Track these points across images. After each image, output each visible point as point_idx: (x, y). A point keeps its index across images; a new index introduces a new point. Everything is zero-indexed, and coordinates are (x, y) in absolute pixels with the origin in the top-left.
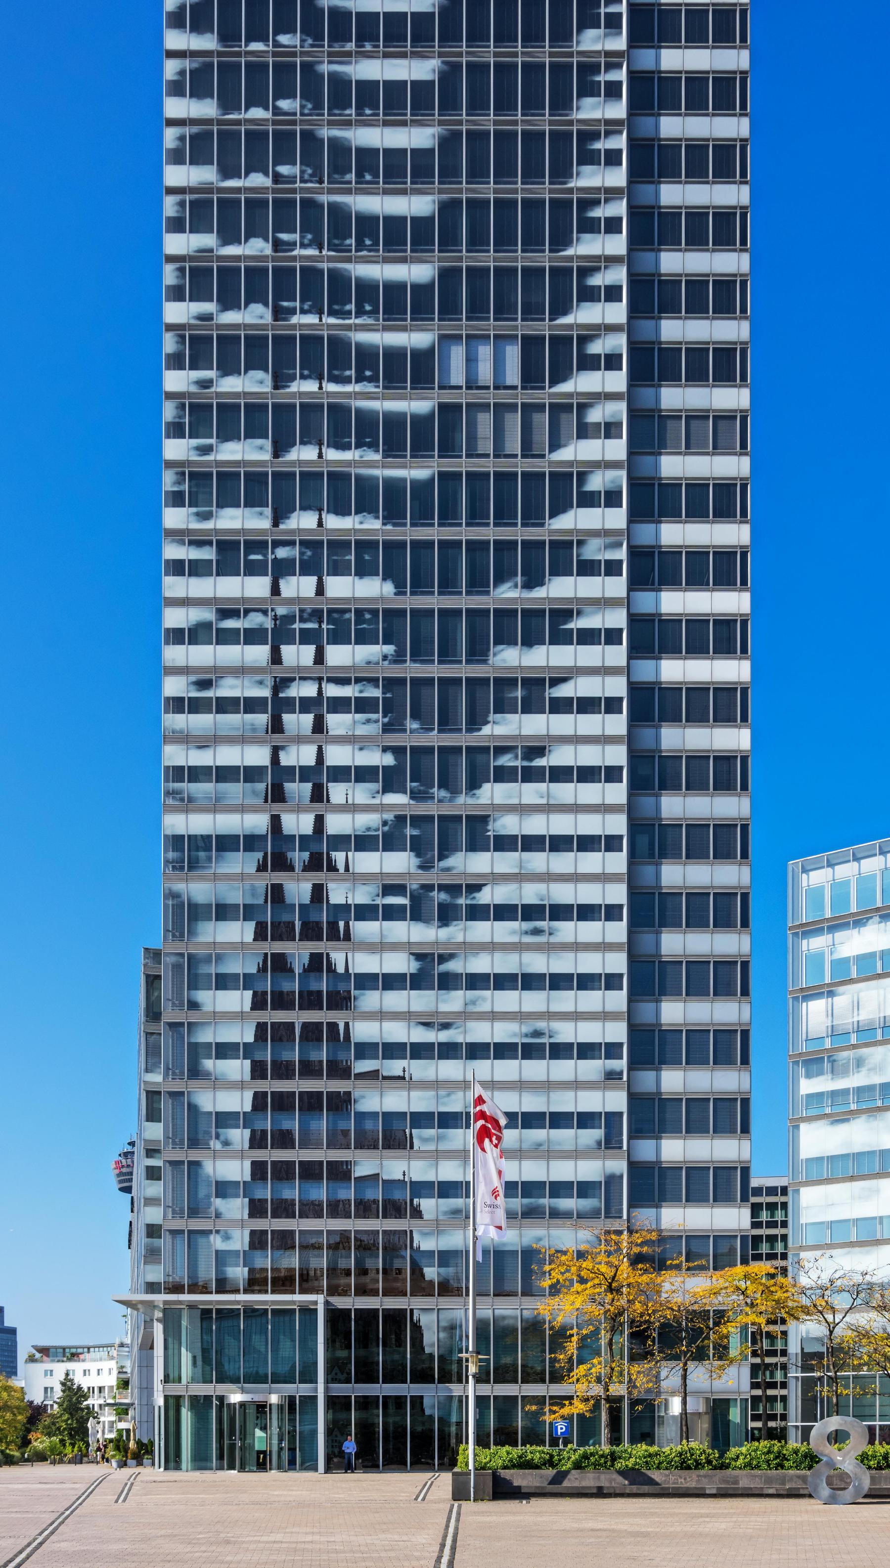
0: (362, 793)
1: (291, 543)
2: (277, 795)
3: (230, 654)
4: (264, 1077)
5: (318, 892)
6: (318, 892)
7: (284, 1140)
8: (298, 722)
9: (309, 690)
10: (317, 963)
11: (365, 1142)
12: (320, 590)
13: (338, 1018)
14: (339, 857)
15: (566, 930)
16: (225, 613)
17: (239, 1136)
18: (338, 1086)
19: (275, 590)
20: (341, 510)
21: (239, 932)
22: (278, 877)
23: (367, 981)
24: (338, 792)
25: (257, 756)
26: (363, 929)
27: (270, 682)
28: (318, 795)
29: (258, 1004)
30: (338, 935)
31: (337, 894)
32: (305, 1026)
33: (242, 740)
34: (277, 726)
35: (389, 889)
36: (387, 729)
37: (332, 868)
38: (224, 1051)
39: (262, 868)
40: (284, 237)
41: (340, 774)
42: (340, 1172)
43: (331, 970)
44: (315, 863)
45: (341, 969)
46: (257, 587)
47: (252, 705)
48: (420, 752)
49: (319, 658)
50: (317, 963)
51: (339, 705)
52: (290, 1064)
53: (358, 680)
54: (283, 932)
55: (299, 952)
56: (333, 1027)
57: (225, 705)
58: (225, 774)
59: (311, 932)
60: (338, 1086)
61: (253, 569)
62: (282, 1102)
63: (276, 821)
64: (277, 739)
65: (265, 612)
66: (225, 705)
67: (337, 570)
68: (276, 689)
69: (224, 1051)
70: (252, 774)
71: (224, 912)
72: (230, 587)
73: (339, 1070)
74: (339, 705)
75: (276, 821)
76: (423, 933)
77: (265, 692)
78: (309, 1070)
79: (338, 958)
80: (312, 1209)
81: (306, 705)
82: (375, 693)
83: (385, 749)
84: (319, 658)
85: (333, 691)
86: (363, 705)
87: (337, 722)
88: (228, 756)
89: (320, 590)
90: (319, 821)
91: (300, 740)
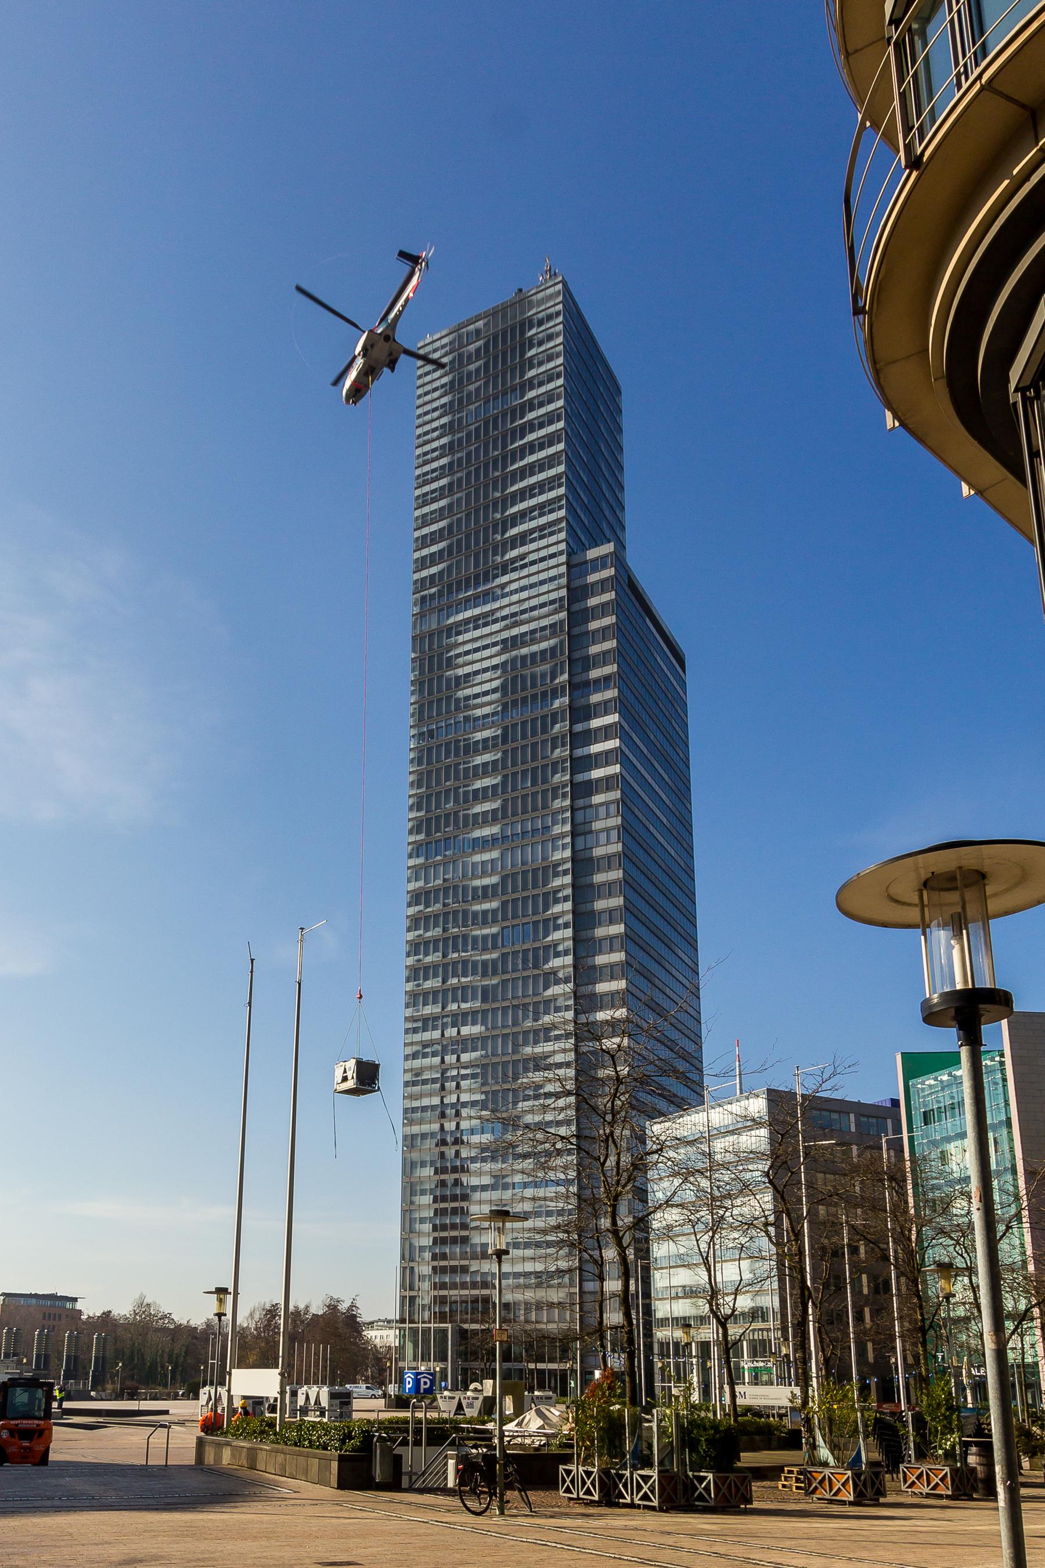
1: (448, 1016)
2: (443, 1115)
3: (427, 1061)
5: (457, 1153)
6: (457, 1153)
7: (444, 1256)
8: (451, 1085)
9: (454, 1073)
12: (459, 1032)
13: (464, 1204)
14: (465, 1138)
15: (479, 678)
16: (425, 1046)
19: (443, 1035)
20: (465, 1000)
21: (428, 1171)
22: (443, 1149)
24: (464, 1112)
25: (436, 1101)
26: (474, 1167)
28: (458, 1114)
29: (435, 1201)
30: (464, 1170)
31: (464, 1155)
32: (452, 1208)
33: (430, 1095)
34: (443, 1088)
36: (483, 1084)
37: (462, 1142)
39: (437, 1145)
41: (465, 1105)
43: (462, 1185)
44: (457, 1141)
46: (436, 1034)
47: (434, 1081)
48: (495, 1093)
50: (457, 1182)
51: (465, 1077)
52: (446, 1225)
54: (444, 1170)
55: (450, 1178)
57: (425, 1082)
58: (424, 1109)
59: (455, 1169)
61: (434, 1028)
62: (443, 1241)
63: (442, 1126)
64: (443, 1093)
66: (425, 1082)
67: (464, 1024)
68: (442, 1074)
70: (433, 1108)
71: (423, 1164)
72: (427, 1036)
74: (465, 1077)
75: (442, 1126)
78: (454, 1226)
79: (464, 1180)
81: (453, 1078)
83: (482, 1093)
85: (463, 1072)
86: (474, 1076)
87: (464, 1084)
88: (426, 1102)
89: (459, 1032)
90: (458, 1124)
91: (451, 1093)
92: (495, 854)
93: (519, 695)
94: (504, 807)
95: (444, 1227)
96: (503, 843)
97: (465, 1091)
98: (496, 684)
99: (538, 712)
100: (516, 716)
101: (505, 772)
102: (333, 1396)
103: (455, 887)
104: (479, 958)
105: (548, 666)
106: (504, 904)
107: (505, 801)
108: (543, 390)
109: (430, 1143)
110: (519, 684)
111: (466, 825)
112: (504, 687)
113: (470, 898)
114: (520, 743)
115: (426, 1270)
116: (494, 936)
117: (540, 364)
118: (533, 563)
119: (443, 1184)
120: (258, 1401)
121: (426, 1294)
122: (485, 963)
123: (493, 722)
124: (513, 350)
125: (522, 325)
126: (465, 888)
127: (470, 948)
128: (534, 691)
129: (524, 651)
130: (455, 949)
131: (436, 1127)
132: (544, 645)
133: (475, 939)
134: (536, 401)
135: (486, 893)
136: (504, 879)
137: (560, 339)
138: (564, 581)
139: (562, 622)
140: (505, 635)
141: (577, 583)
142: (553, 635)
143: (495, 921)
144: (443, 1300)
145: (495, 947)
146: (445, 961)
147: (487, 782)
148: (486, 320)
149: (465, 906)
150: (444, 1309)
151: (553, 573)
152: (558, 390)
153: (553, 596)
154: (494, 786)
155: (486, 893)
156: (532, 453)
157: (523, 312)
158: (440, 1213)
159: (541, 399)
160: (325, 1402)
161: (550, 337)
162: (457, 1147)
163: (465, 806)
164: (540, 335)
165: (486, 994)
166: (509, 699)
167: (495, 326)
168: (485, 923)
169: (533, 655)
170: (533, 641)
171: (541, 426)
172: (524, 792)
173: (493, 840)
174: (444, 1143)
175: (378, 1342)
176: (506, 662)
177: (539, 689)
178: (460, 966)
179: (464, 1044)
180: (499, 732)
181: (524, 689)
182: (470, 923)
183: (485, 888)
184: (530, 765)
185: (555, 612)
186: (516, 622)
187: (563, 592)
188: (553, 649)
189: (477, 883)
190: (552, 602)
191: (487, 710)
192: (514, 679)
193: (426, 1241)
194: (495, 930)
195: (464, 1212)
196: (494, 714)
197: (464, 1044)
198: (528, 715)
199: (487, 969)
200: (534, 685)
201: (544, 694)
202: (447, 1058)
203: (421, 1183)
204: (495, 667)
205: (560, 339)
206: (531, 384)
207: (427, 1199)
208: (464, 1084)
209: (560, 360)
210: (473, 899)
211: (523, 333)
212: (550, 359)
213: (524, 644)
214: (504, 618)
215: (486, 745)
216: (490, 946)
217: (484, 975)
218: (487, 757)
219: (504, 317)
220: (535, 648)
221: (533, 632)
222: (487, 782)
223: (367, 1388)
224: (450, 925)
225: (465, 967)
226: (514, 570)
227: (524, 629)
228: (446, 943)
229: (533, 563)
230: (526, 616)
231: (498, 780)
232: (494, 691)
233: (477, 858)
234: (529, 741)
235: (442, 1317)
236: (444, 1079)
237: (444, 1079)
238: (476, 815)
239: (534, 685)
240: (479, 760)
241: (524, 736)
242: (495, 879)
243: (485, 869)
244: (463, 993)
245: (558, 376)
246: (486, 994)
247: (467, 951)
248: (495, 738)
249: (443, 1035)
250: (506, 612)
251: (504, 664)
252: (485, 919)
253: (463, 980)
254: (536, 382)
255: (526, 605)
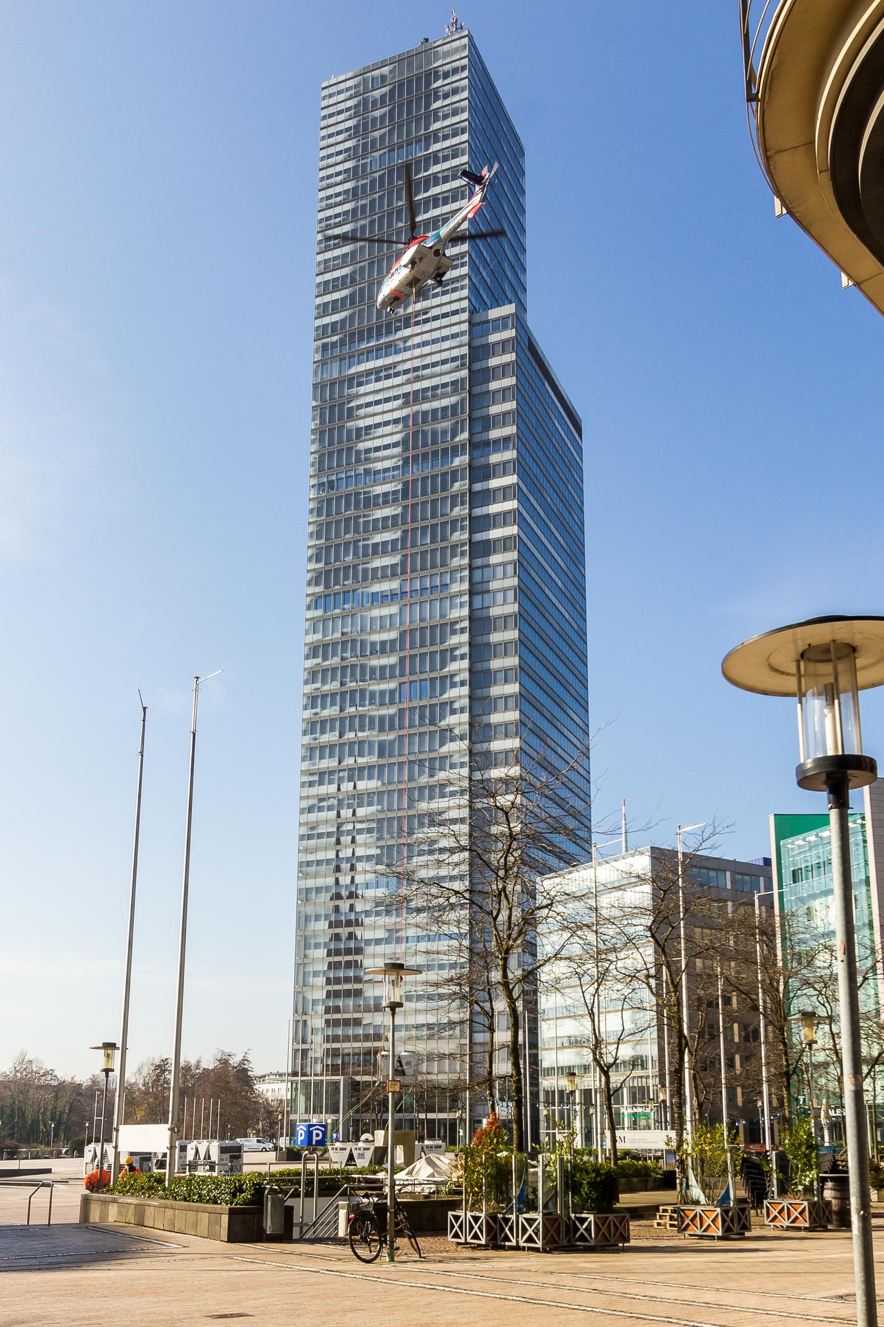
0: (368, 866)
1: (345, 770)
2: (338, 869)
4: (330, 984)
5: (352, 907)
6: (352, 907)
7: (337, 1010)
8: (346, 839)
9: (350, 827)
10: (351, 936)
11: (367, 1010)
12: (355, 787)
13: (358, 958)
14: (359, 892)
17: (321, 1009)
18: (358, 986)
19: (339, 789)
21: (323, 925)
22: (338, 902)
23: (368, 942)
24: (359, 866)
25: (331, 855)
26: (367, 921)
27: (336, 825)
28: (353, 868)
29: (329, 954)
30: (358, 923)
31: (359, 907)
34: (338, 842)
35: (378, 904)
38: (316, 974)
39: (332, 899)
40: (344, 655)
41: (359, 859)
42: (357, 1022)
43: (356, 938)
44: (351, 895)
45: (359, 938)
46: (333, 788)
47: (329, 835)
49: (354, 814)
50: (351, 936)
51: (360, 831)
53: (368, 821)
55: (344, 932)
56: (356, 961)
59: (349, 923)
60: (358, 986)
62: (337, 994)
63: (337, 880)
64: (338, 847)
65: (334, 798)
67: (361, 778)
68: (338, 828)
69: (316, 974)
70: (328, 862)
71: (317, 918)
73: (358, 980)
74: (360, 831)
75: (337, 880)
76: (390, 920)
77: (335, 829)
78: (347, 980)
80: (347, 1039)
81: (349, 832)
82: (374, 825)
84: (354, 814)
85: (359, 826)
86: (369, 831)
87: (360, 838)
89: (355, 787)
90: (353, 878)
92: (394, 609)
93: (421, 451)
94: (403, 563)
95: (337, 981)
96: (402, 598)
97: (361, 845)
98: (397, 438)
99: (438, 470)
100: (416, 472)
101: (405, 527)
102: (223, 1150)
103: (354, 641)
104: (376, 713)
105: (449, 423)
106: (402, 660)
107: (405, 556)
108: (447, 143)
109: (325, 897)
110: (419, 443)
111: (365, 579)
112: (404, 442)
113: (368, 653)
114: (420, 499)
115: (318, 1022)
116: (392, 692)
117: (445, 117)
118: (435, 318)
119: (337, 937)
120: (146, 1157)
121: (318, 1047)
122: (382, 719)
123: (393, 476)
124: (419, 100)
125: (428, 75)
126: (363, 643)
127: (367, 702)
128: (434, 448)
129: (426, 407)
130: (353, 704)
131: (331, 881)
132: (445, 402)
133: (372, 694)
134: (440, 155)
135: (384, 648)
136: (402, 634)
137: (465, 94)
138: (465, 339)
139: (463, 380)
140: (407, 389)
141: (477, 342)
142: (455, 392)
143: (392, 677)
144: (335, 1053)
145: (392, 702)
146: (343, 715)
147: (387, 536)
148: (392, 66)
149: (363, 661)
150: (337, 1062)
151: (455, 330)
152: (463, 146)
153: (455, 353)
154: (394, 541)
155: (384, 648)
156: (435, 206)
157: (429, 63)
158: (332, 966)
159: (446, 152)
160: (215, 1157)
161: (455, 91)
162: (351, 901)
163: (365, 559)
164: (446, 88)
165: (383, 749)
166: (410, 453)
167: (401, 73)
168: (382, 678)
169: (434, 411)
170: (435, 397)
171: (446, 180)
172: (423, 549)
173: (392, 595)
174: (338, 896)
175: (270, 1096)
176: (408, 416)
177: (440, 446)
178: (357, 720)
179: (360, 799)
180: (400, 487)
181: (425, 445)
182: (368, 677)
183: (383, 643)
184: (430, 522)
185: (457, 369)
186: (418, 377)
187: (465, 350)
188: (454, 407)
189: (376, 638)
190: (454, 359)
191: (388, 464)
192: (415, 433)
193: (321, 995)
194: (393, 685)
195: (357, 965)
196: (395, 468)
197: (360, 799)
198: (428, 472)
199: (383, 724)
200: (434, 442)
201: (444, 451)
202: (343, 813)
203: (315, 936)
204: (396, 421)
205: (465, 94)
206: (435, 137)
207: (322, 953)
208: (360, 838)
209: (465, 115)
210: (371, 654)
211: (428, 84)
212: (455, 113)
213: (425, 399)
214: (406, 372)
215: (387, 499)
216: (387, 702)
217: (381, 729)
218: (387, 512)
219: (410, 65)
220: (436, 404)
221: (434, 388)
222: (387, 536)
223: (258, 1141)
224: (348, 679)
225: (362, 722)
226: (417, 323)
227: (426, 384)
228: (345, 697)
229: (435, 318)
230: (425, 372)
231: (398, 535)
232: (395, 445)
233: (376, 613)
234: (429, 497)
235: (334, 1070)
236: (339, 832)
237: (339, 832)
238: (375, 570)
239: (434, 442)
240: (379, 514)
241: (424, 493)
242: (393, 635)
243: (383, 624)
244: (359, 747)
245: (463, 131)
246: (383, 749)
247: (364, 706)
248: (395, 493)
249: (339, 789)
250: (408, 366)
251: (405, 419)
252: (383, 673)
253: (360, 734)
254: (440, 135)
255: (428, 361)
